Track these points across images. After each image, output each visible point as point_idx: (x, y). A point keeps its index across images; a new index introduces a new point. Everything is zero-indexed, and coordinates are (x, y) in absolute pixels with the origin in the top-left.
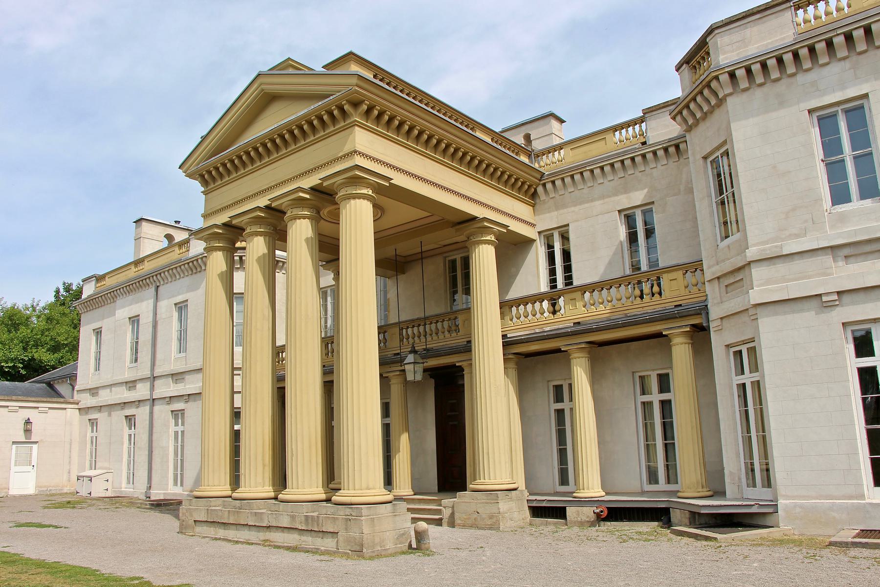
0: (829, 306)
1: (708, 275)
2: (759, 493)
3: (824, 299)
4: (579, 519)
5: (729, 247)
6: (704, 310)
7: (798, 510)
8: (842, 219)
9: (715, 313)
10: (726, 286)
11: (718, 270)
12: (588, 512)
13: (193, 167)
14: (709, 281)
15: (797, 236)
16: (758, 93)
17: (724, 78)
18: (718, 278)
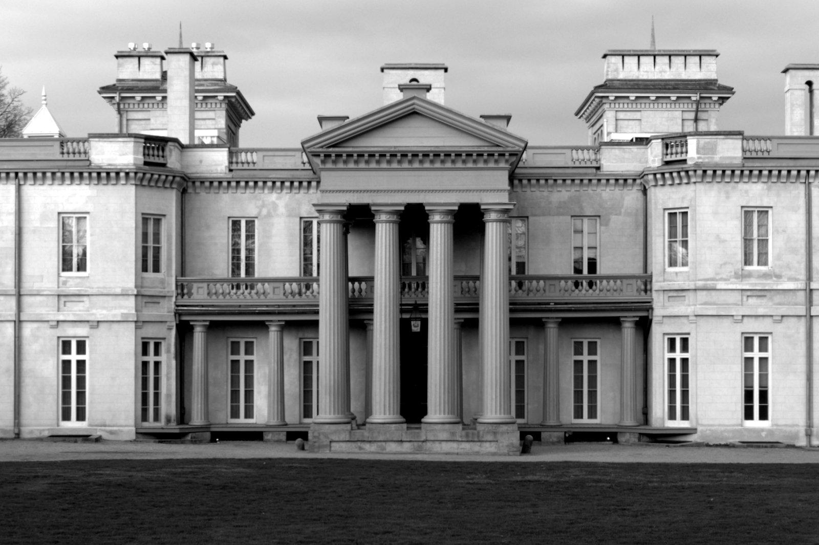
0: (736, 322)
1: (656, 285)
2: (678, 424)
3: (735, 318)
4: (551, 440)
5: (677, 273)
6: (650, 309)
7: (708, 432)
8: (749, 275)
9: (658, 312)
10: (669, 297)
11: (665, 285)
12: (558, 435)
13: (322, 147)
14: (656, 291)
15: (725, 280)
16: (716, 187)
17: (700, 172)
18: (664, 291)
